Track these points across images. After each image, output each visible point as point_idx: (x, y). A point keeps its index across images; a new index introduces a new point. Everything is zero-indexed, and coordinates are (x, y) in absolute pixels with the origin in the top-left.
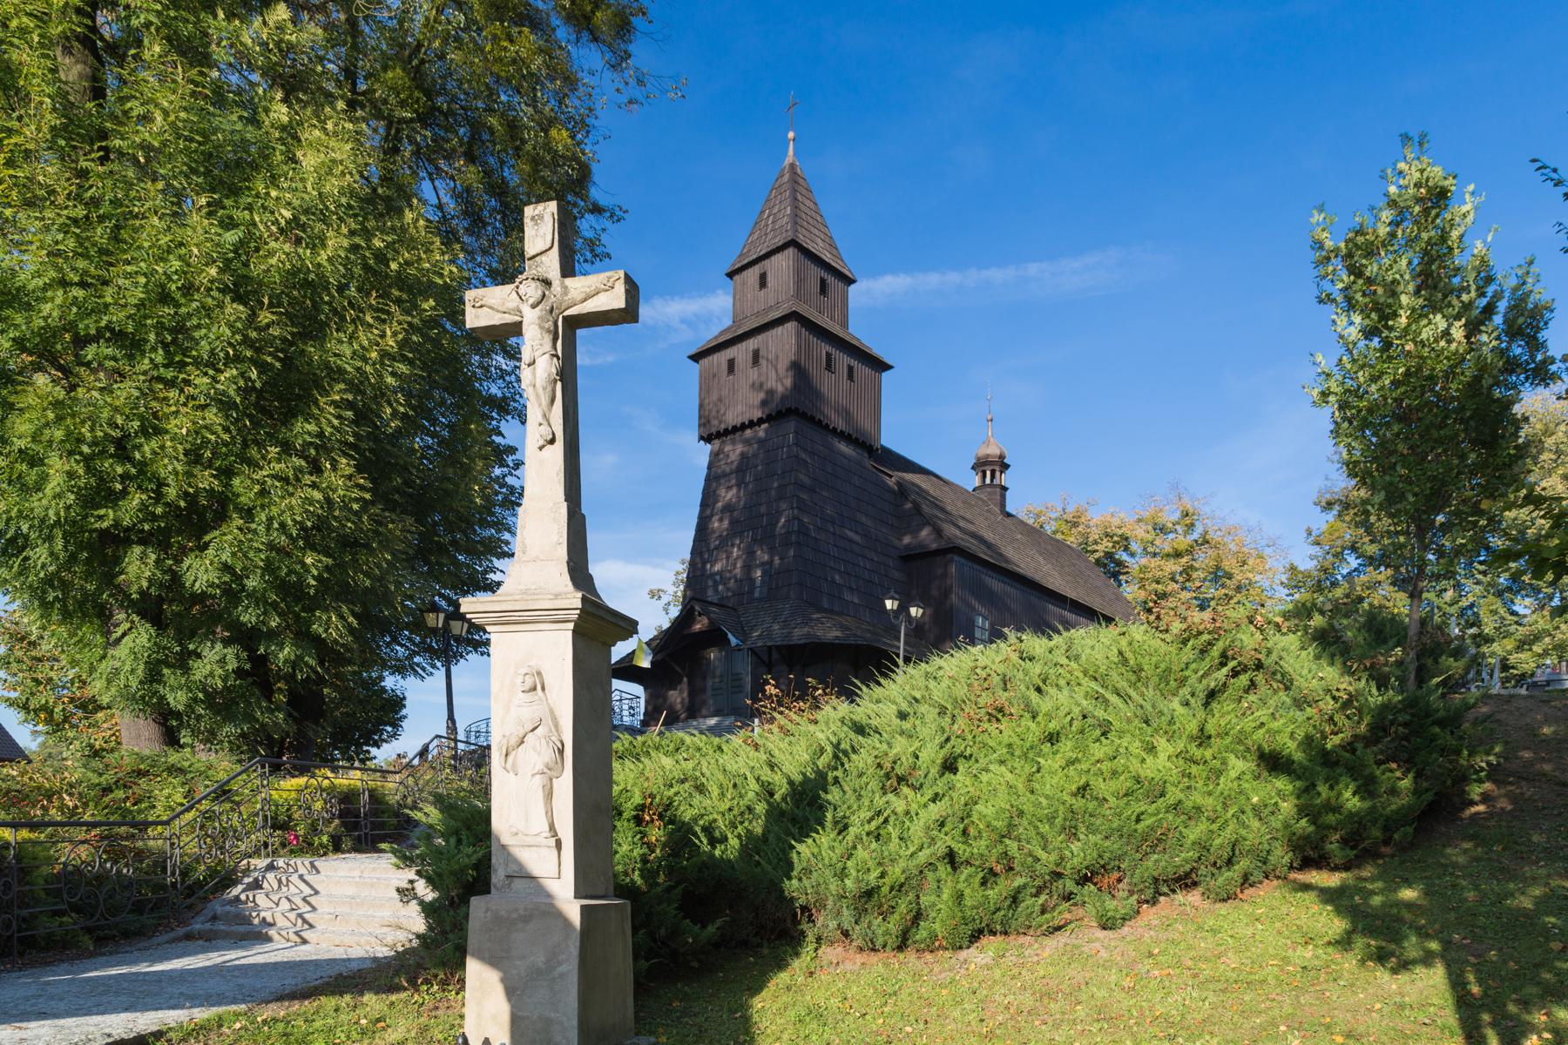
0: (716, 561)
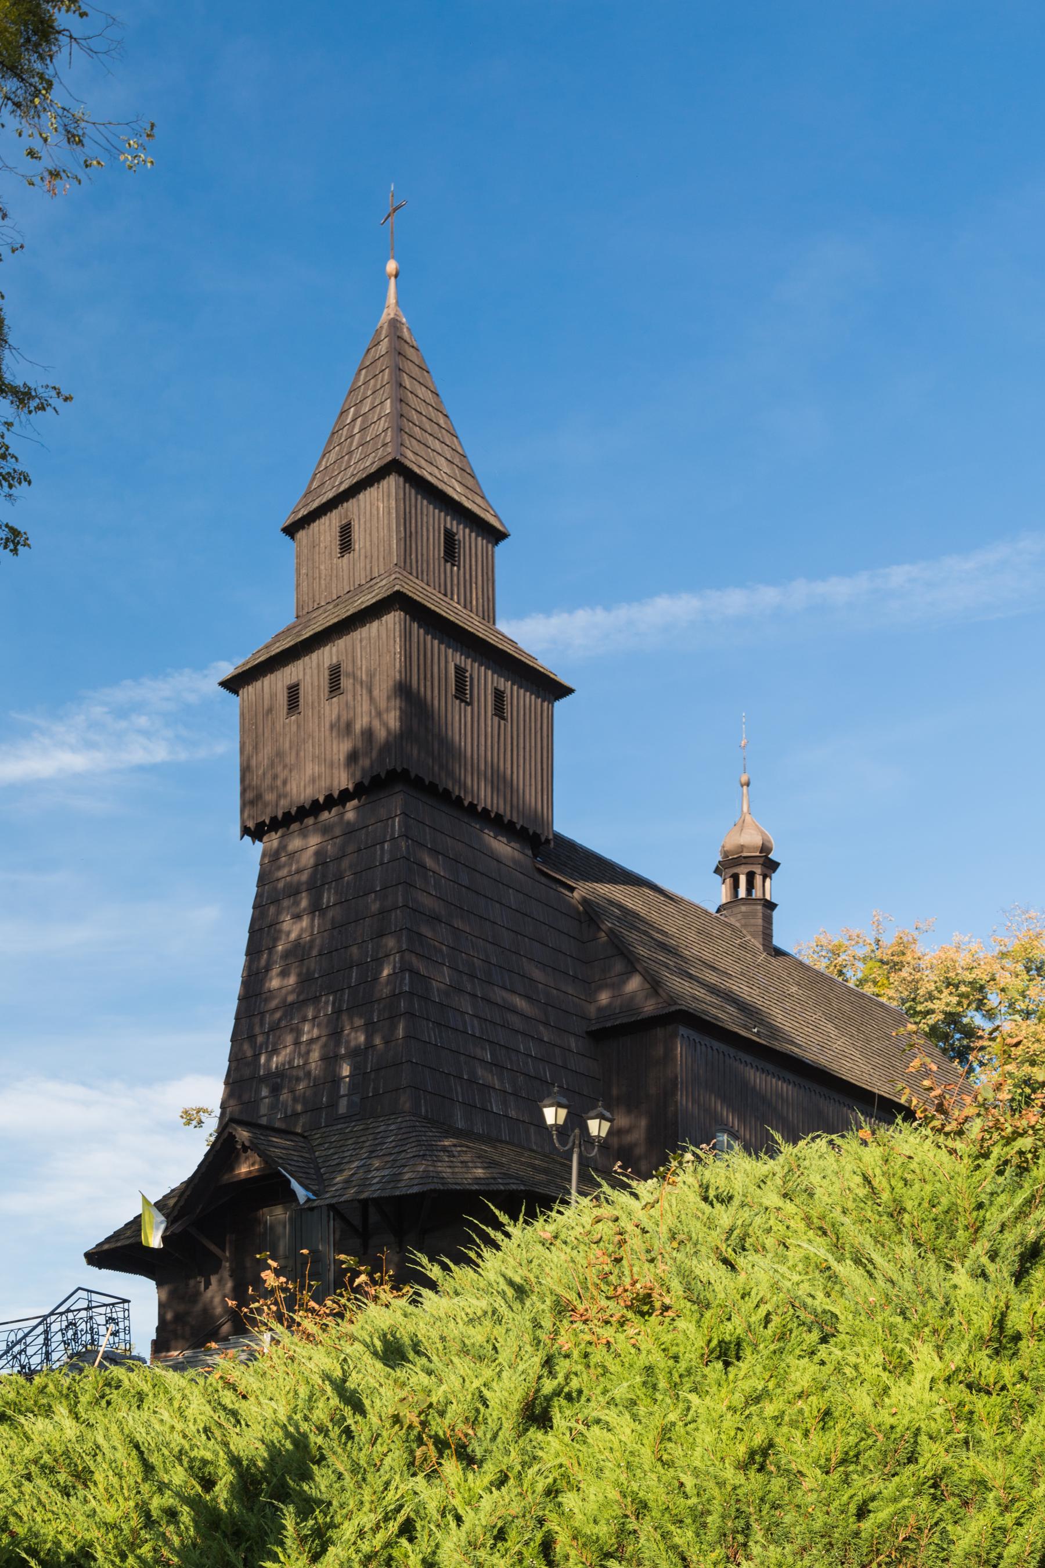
0: (275, 1051)
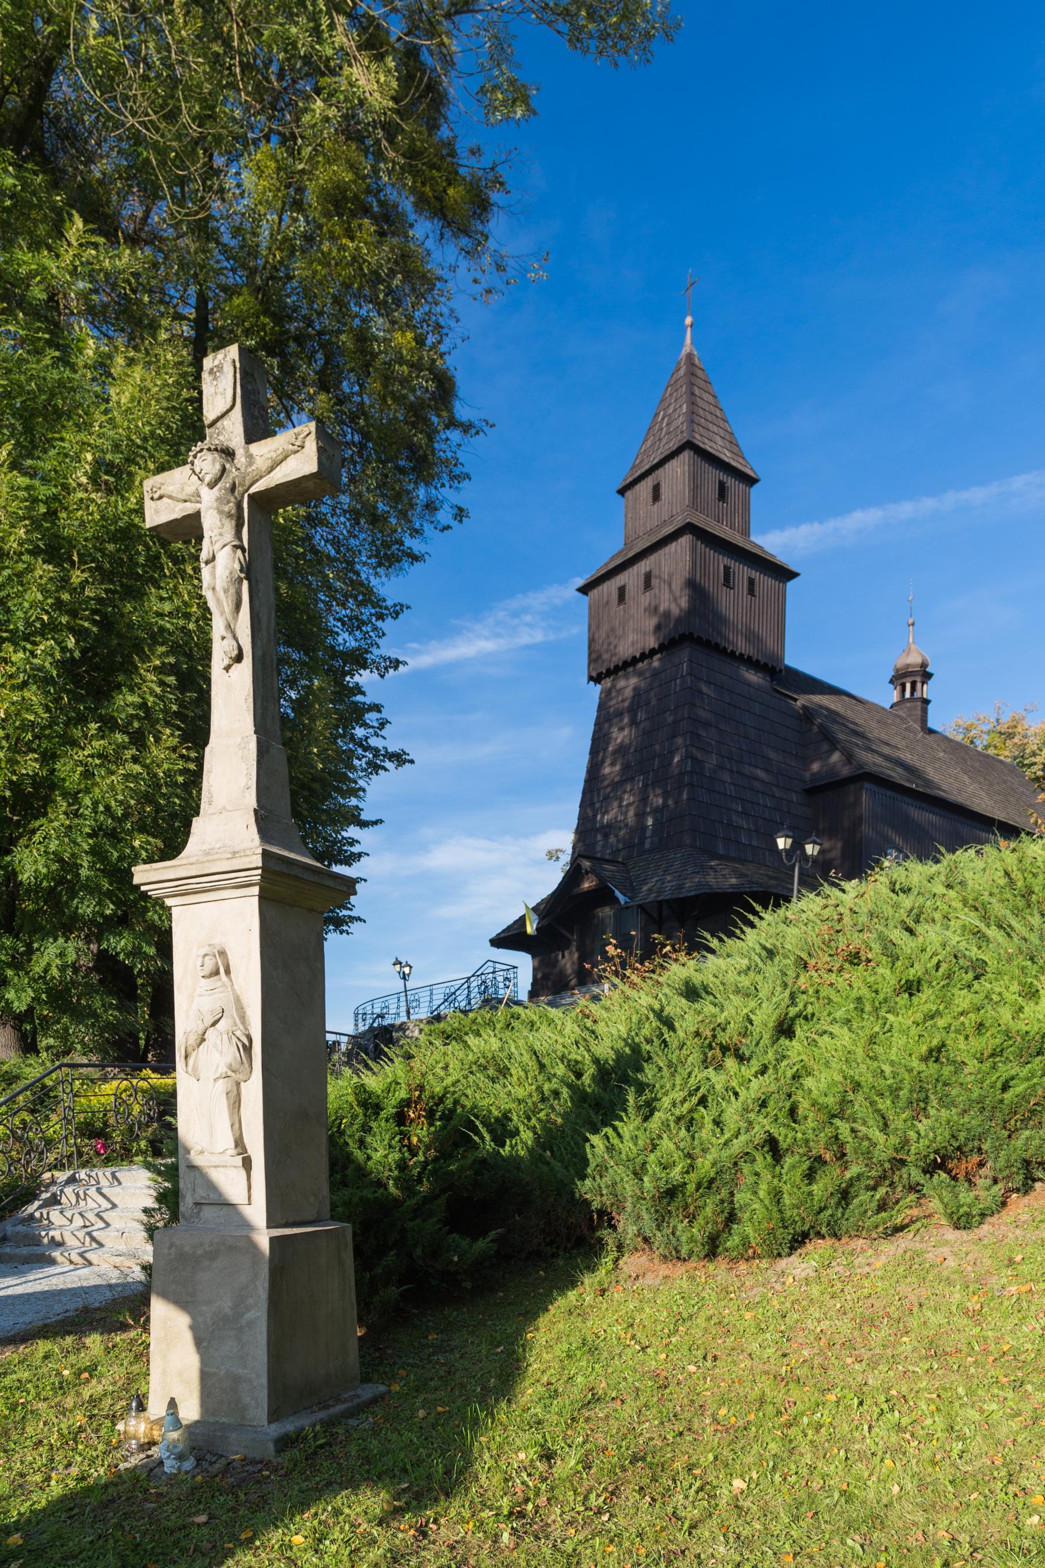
0: (607, 812)
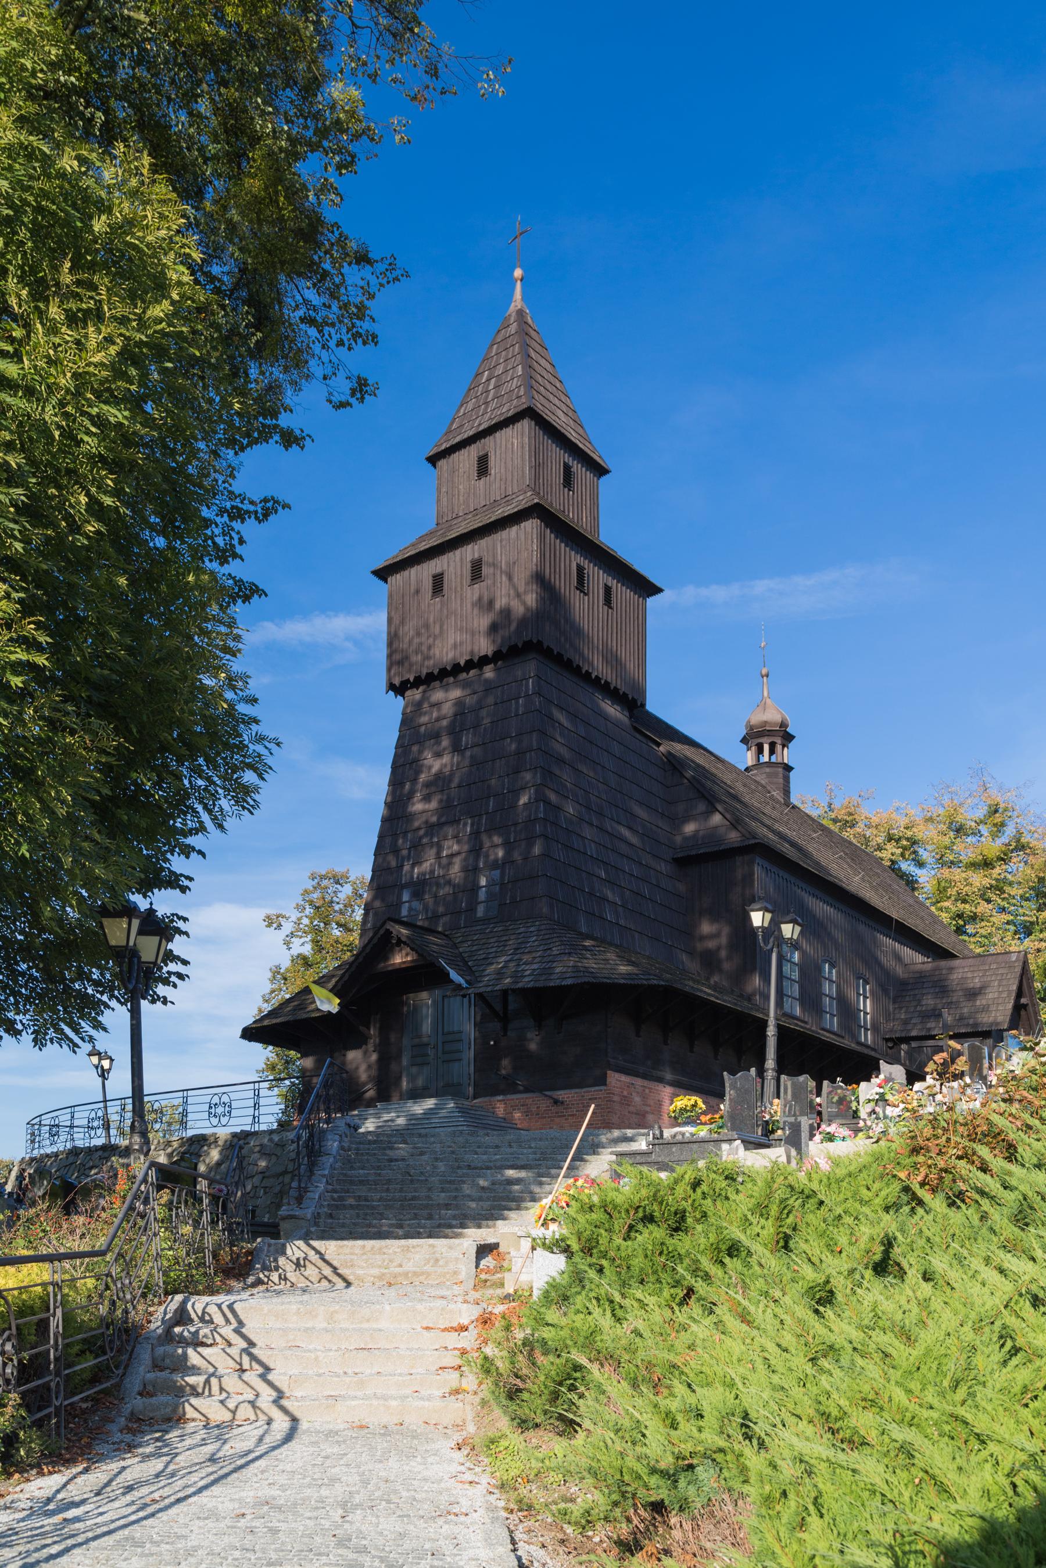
0: (417, 863)
